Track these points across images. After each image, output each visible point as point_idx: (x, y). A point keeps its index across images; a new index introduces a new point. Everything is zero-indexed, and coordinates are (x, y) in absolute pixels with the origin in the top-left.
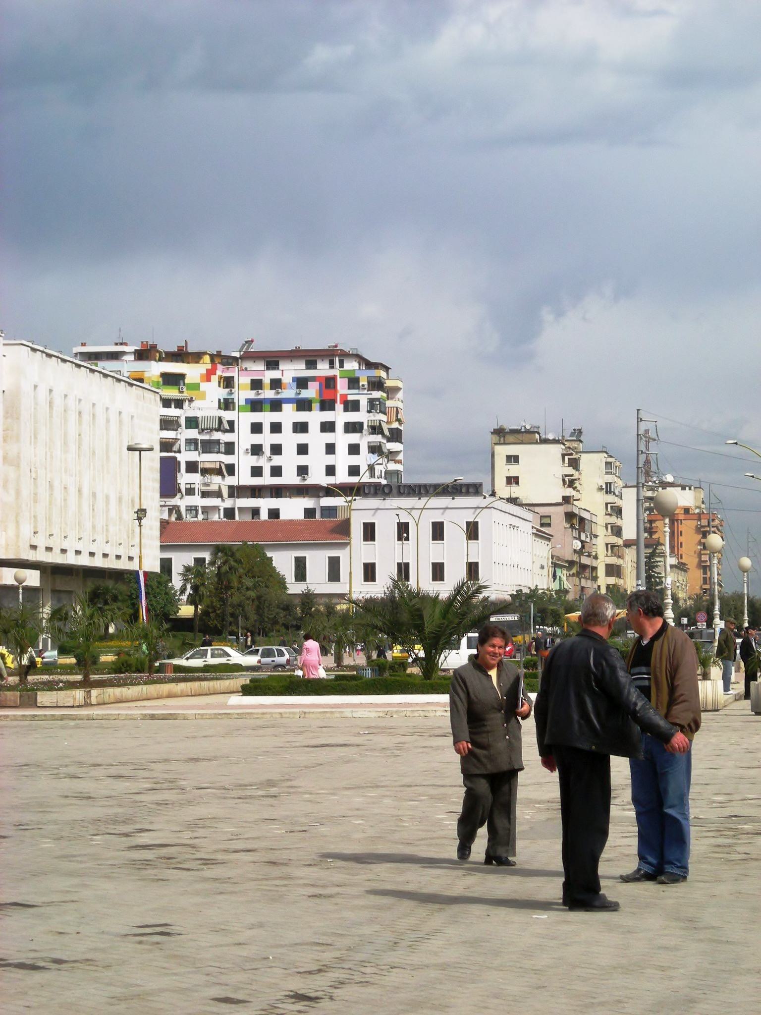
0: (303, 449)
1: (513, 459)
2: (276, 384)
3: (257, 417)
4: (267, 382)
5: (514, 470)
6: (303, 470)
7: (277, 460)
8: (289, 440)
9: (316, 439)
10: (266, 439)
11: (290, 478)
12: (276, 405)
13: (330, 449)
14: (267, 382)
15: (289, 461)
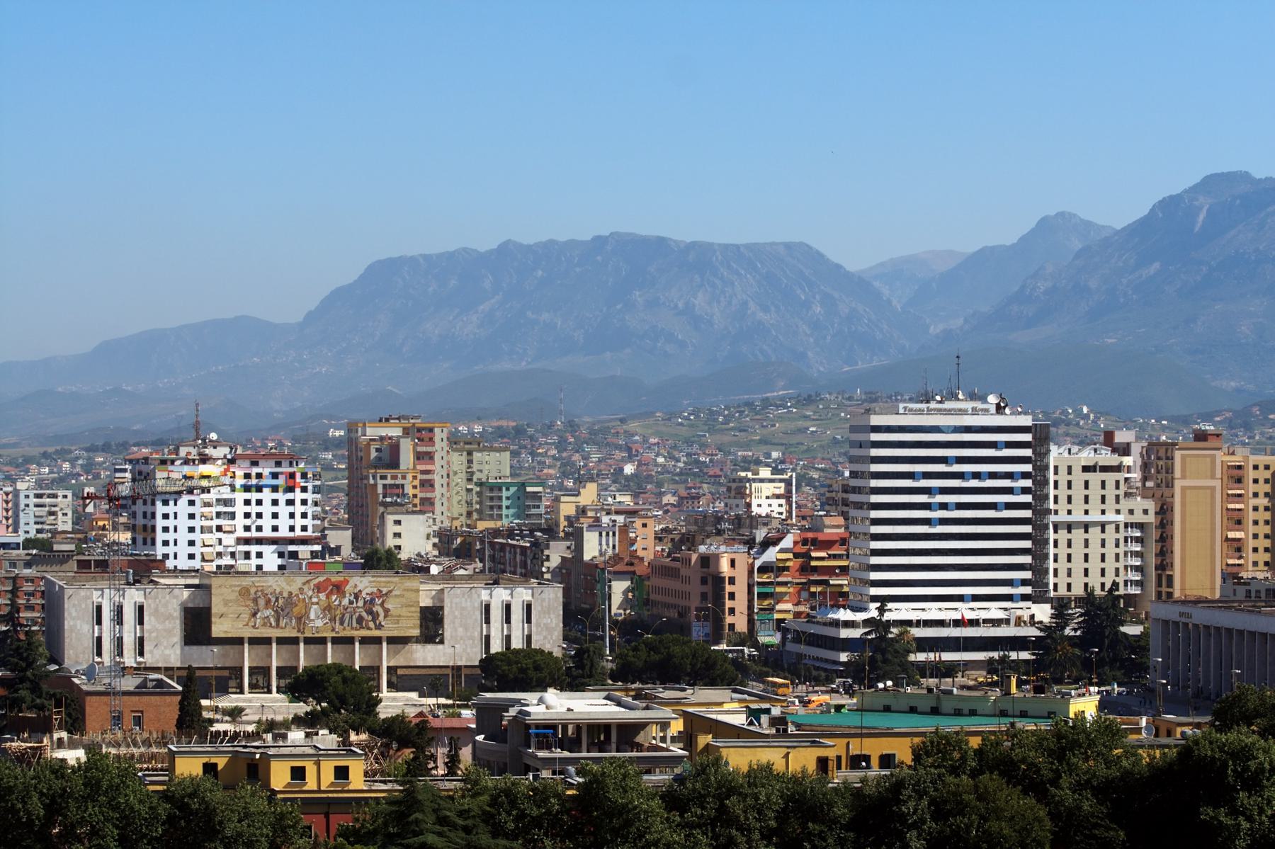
0: (275, 516)
1: (398, 522)
2: (259, 476)
3: (247, 496)
4: (254, 474)
5: (397, 529)
6: (275, 529)
7: (259, 522)
8: (267, 509)
9: (283, 510)
10: (254, 509)
11: (267, 533)
12: (259, 489)
13: (292, 515)
14: (254, 474)
15: (267, 522)
